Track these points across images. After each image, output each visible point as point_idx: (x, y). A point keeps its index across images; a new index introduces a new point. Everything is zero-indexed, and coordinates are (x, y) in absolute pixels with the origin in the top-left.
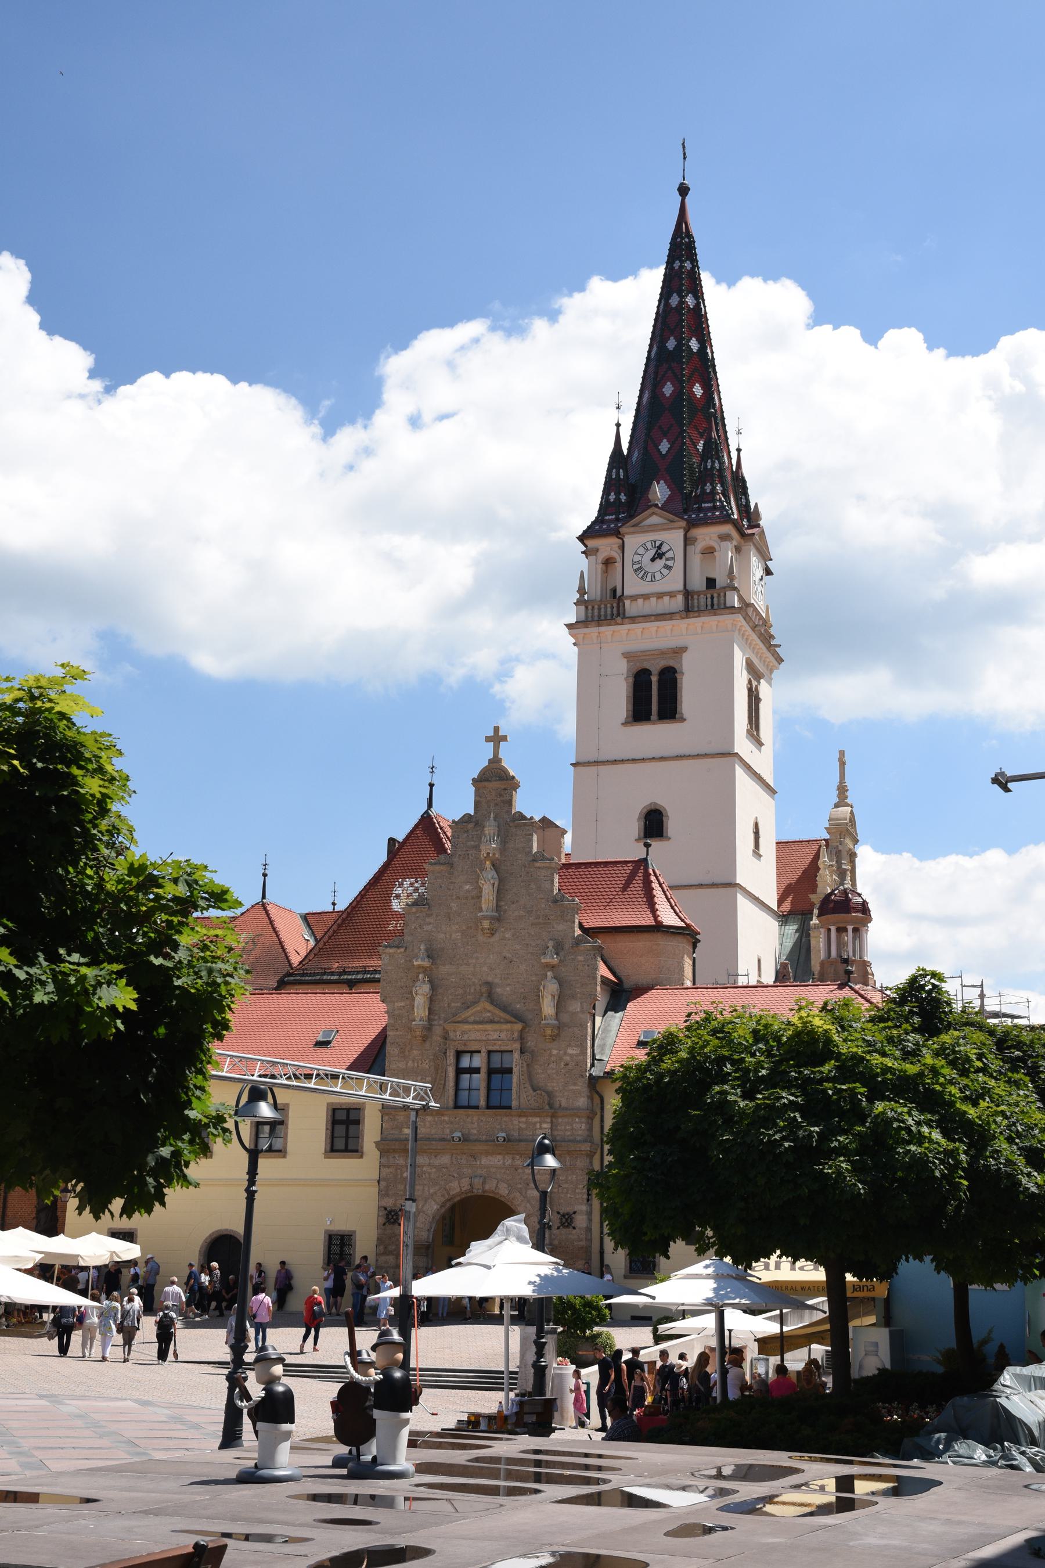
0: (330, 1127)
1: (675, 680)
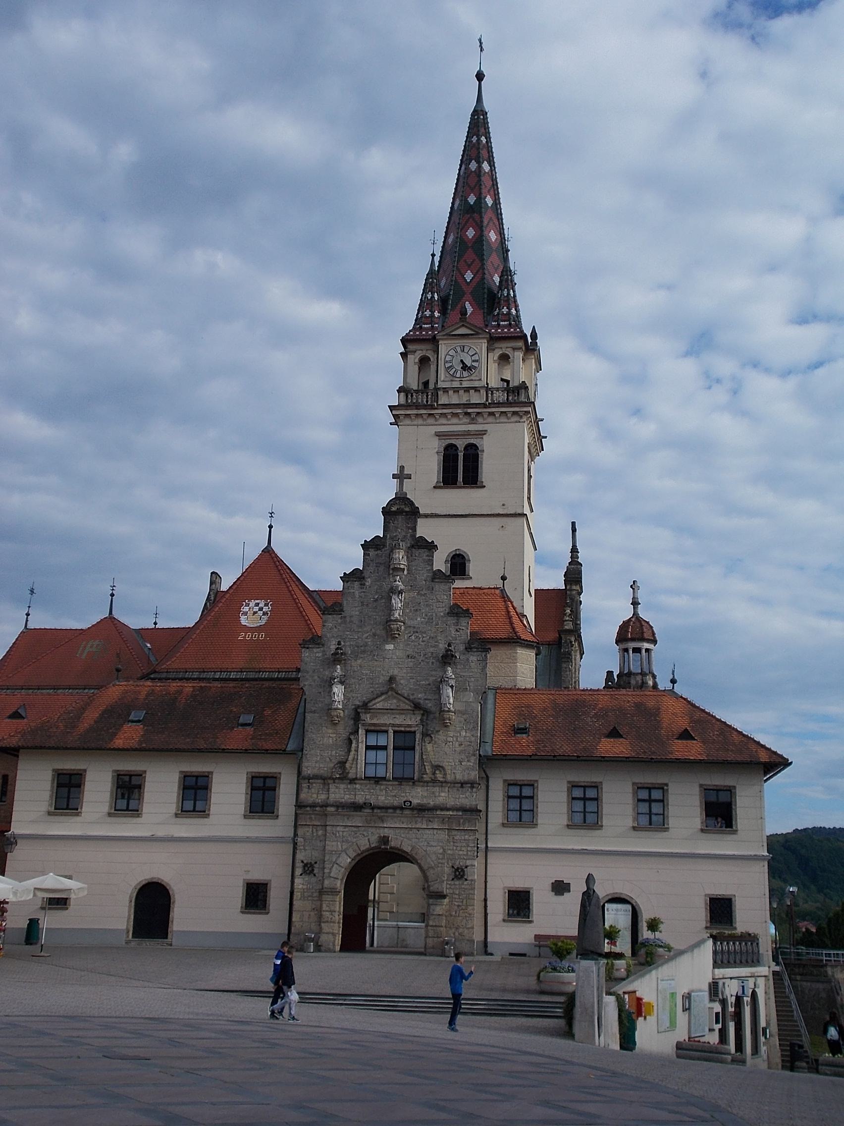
1: (478, 454)
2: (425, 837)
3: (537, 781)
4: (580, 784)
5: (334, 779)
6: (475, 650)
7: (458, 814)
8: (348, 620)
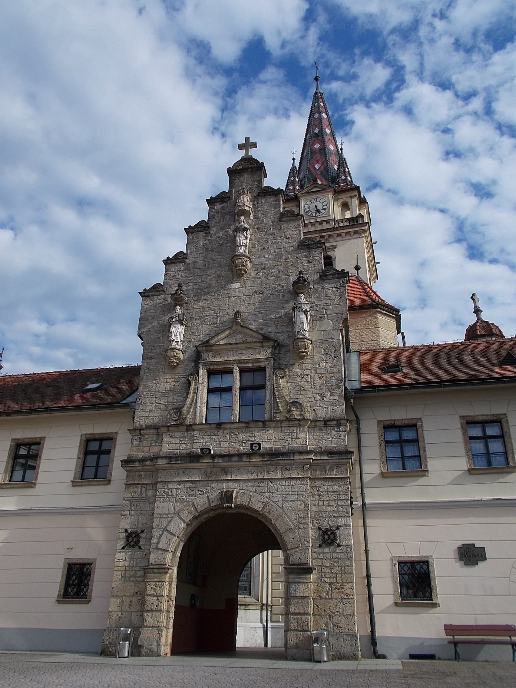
0: (82, 457)
2: (280, 489)
3: (420, 419)
4: (477, 419)
5: (168, 427)
6: (331, 276)
7: (322, 458)
8: (191, 267)
